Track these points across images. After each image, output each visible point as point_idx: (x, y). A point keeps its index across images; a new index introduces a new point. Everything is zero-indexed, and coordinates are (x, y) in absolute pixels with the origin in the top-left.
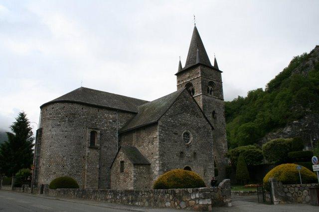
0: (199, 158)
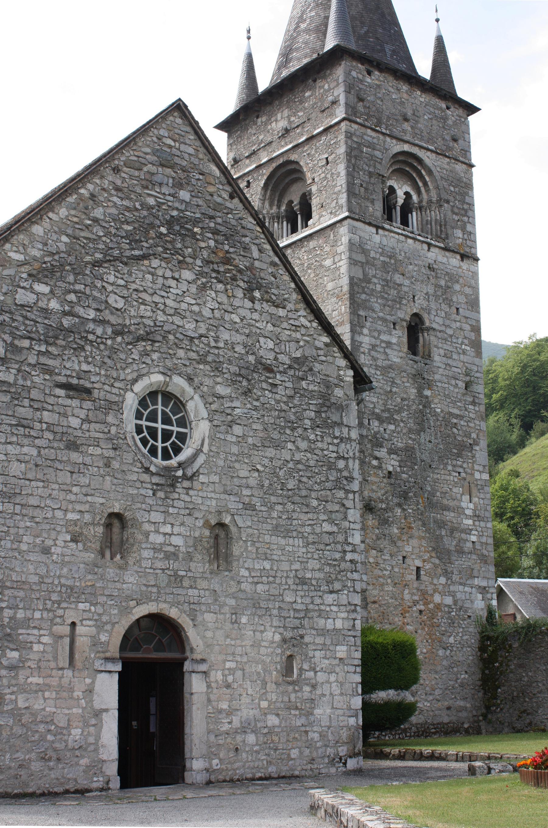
0: (247, 564)
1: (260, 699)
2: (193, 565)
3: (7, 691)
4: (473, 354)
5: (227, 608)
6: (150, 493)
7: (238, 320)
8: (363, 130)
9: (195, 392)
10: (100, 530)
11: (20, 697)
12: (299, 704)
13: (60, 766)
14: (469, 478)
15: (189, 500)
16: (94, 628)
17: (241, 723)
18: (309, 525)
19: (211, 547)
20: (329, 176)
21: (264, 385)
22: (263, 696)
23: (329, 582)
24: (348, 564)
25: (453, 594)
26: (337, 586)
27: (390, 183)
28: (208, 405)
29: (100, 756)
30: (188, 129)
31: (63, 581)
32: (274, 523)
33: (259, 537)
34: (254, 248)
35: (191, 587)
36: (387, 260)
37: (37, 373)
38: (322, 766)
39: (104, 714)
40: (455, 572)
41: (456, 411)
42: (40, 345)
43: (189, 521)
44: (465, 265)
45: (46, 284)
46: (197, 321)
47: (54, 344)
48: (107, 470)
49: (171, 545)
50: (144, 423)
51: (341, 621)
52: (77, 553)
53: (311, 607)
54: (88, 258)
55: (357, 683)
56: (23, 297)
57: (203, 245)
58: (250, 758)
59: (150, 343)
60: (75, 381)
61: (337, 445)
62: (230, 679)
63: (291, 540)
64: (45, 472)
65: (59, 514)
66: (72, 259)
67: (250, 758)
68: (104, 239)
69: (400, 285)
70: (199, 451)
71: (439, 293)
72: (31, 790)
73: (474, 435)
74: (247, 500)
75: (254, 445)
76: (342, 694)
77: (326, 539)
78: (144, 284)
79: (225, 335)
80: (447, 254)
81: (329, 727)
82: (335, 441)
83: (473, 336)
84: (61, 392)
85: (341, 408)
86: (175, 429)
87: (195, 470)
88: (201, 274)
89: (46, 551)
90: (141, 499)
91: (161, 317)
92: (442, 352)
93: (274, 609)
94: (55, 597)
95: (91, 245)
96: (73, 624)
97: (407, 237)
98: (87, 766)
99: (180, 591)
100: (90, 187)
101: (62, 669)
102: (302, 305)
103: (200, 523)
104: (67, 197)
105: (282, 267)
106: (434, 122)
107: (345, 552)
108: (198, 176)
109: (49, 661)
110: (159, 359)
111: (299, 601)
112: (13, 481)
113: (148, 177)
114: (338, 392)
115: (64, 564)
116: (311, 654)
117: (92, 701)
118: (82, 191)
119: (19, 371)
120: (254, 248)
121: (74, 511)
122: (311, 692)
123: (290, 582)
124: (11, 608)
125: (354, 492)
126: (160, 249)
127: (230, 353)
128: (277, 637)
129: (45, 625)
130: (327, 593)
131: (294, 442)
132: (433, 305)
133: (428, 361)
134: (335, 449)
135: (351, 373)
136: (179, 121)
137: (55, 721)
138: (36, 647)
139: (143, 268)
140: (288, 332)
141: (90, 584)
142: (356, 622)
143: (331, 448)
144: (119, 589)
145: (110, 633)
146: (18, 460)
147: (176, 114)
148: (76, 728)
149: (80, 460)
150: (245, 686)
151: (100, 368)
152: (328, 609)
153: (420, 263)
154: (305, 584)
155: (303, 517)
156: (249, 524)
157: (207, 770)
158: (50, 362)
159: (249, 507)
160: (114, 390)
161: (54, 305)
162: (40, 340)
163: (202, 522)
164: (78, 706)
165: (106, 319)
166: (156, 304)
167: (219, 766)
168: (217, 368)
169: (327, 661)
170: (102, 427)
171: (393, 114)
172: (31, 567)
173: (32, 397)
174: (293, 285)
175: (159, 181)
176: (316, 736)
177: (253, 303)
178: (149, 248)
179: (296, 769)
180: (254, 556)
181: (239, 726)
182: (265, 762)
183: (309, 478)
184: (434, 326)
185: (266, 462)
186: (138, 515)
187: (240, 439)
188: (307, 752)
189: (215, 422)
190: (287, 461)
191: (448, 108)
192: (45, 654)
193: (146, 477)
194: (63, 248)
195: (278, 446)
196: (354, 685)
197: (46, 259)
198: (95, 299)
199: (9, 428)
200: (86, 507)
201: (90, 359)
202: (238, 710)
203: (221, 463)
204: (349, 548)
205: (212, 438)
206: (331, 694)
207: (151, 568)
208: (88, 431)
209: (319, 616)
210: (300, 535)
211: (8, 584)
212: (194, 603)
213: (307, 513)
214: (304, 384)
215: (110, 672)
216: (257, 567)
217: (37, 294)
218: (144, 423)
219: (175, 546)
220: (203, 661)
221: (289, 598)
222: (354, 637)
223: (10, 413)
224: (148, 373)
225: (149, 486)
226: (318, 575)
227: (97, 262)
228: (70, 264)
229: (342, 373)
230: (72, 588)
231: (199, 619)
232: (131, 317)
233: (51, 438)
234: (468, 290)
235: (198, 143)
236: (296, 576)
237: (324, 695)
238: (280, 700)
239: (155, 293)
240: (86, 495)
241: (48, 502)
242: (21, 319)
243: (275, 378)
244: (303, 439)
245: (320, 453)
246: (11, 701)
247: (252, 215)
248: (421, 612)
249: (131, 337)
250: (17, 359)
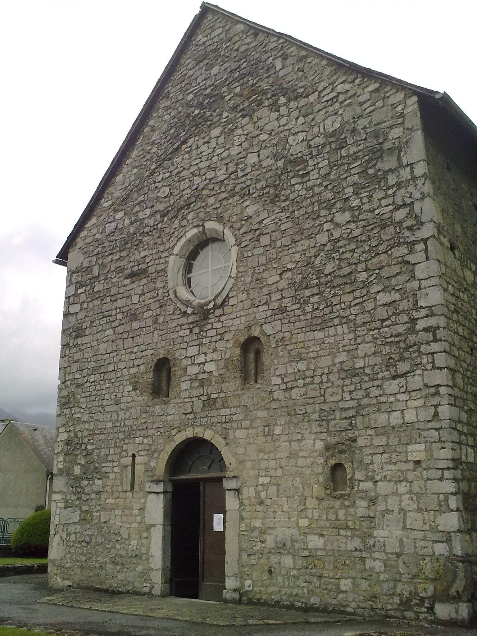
1: (299, 517)
6: (188, 332)
12: (350, 523)
13: (125, 570)
16: (146, 457)
17: (276, 542)
26: (403, 367)
31: (127, 423)
33: (290, 339)
38: (390, 607)
39: (152, 528)
43: (220, 345)
49: (205, 372)
51: (414, 412)
53: (366, 401)
58: (287, 583)
60: (135, 269)
63: (332, 331)
67: (287, 583)
72: (105, 587)
77: (382, 313)
81: (398, 555)
82: (390, 192)
84: (127, 281)
87: (224, 297)
90: (180, 340)
93: (314, 413)
99: (213, 413)
101: (125, 492)
107: (413, 321)
109: (118, 486)
116: (367, 460)
121: (134, 366)
122: (368, 507)
125: (425, 241)
128: (320, 445)
130: (388, 379)
138: (112, 476)
142: (439, 409)
148: (133, 540)
150: (280, 503)
152: (392, 399)
155: (347, 298)
156: (278, 328)
167: (251, 588)
168: (244, 194)
169: (393, 467)
176: (378, 566)
182: (306, 590)
183: (353, 251)
186: (177, 355)
188: (365, 585)
190: (325, 245)
193: (184, 320)
196: (442, 497)
200: (142, 361)
203: (249, 279)
207: (188, 398)
209: (379, 410)
210: (344, 321)
211: (96, 432)
212: (226, 422)
215: (157, 493)
216: (290, 370)
222: (436, 429)
226: (372, 361)
231: (231, 436)
238: (324, 517)
240: (142, 351)
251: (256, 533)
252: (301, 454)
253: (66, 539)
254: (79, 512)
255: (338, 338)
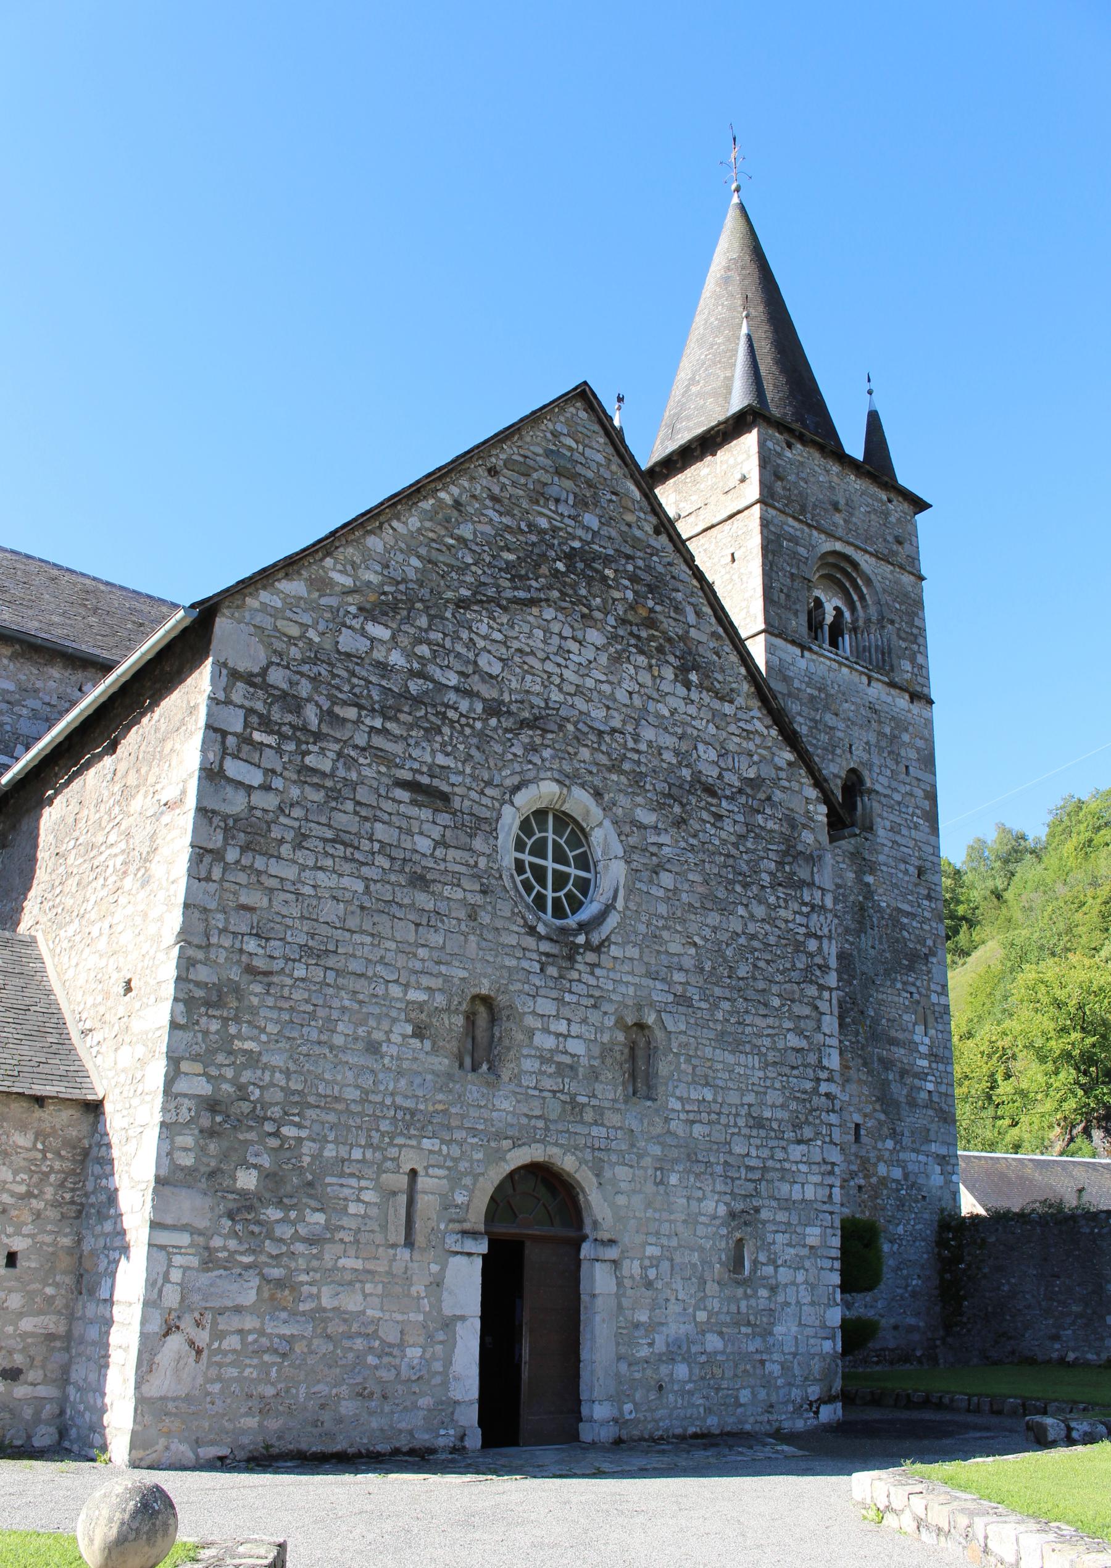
0: (678, 1092)
1: (697, 1308)
2: (599, 1088)
3: (303, 1278)
4: (927, 830)
5: (649, 1159)
7: (667, 714)
8: (782, 517)
9: (605, 816)
10: (459, 1021)
11: (324, 1289)
12: (752, 1318)
14: (923, 1001)
15: (594, 983)
16: (445, 1181)
17: (668, 1345)
18: (768, 1035)
19: (626, 1061)
20: (735, 577)
21: (705, 815)
22: (700, 1304)
23: (797, 1126)
24: (823, 1099)
25: (902, 1163)
26: (808, 1132)
27: (817, 593)
28: (623, 838)
29: (451, 1394)
30: (597, 427)
31: (399, 1100)
32: (719, 1028)
33: (696, 1049)
34: (689, 610)
35: (596, 1123)
36: (816, 693)
37: (368, 761)
40: (907, 1134)
41: (906, 907)
42: (373, 718)
43: (594, 1017)
44: (916, 708)
45: (387, 626)
46: (608, 708)
47: (397, 720)
48: (472, 924)
49: (566, 1053)
50: (527, 858)
51: (812, 1187)
52: (422, 1056)
53: (770, 1163)
54: (449, 595)
55: (835, 1287)
56: (348, 641)
57: (617, 595)
58: (680, 1401)
59: (539, 732)
60: (425, 780)
61: (807, 916)
62: (652, 1273)
63: (743, 1057)
64: (376, 919)
65: (395, 991)
66: (424, 592)
67: (680, 1401)
68: (474, 568)
69: (832, 728)
70: (608, 908)
71: (883, 744)
72: (338, 1448)
73: (929, 942)
74: (679, 990)
75: (690, 905)
76: (812, 1304)
77: (792, 1058)
78: (532, 643)
79: (648, 733)
80: (893, 691)
81: (795, 1355)
82: (805, 909)
83: (926, 805)
84: (404, 795)
85: (812, 859)
86: (573, 871)
88: (614, 638)
89: (373, 1048)
91: (556, 696)
92: (888, 824)
94: (385, 1126)
95: (453, 574)
96: (413, 1173)
97: (840, 664)
98: (429, 1410)
99: (579, 1129)
100: (455, 491)
101: (394, 1246)
102: (755, 703)
103: (610, 1022)
104: (420, 501)
105: (728, 642)
106: (873, 517)
107: (818, 1080)
108: (608, 497)
109: (372, 1231)
110: (553, 757)
111: (754, 1153)
112: (324, 930)
113: (538, 487)
114: (808, 837)
115: (400, 1073)
116: (770, 1238)
117: (440, 1301)
118: (442, 495)
119: (340, 754)
120: (689, 610)
122: (769, 1298)
123: (741, 1122)
124: (314, 1141)
125: (831, 989)
126: (555, 594)
127: (655, 762)
128: (722, 1210)
129: (369, 1172)
130: (793, 1142)
131: (746, 906)
132: (876, 761)
133: (869, 836)
134: (804, 921)
135: (823, 809)
136: (583, 415)
137: (381, 1333)
138: (353, 1208)
139: (531, 619)
140: (736, 740)
141: (440, 1107)
143: (799, 919)
144: (486, 1120)
145: (472, 1192)
146: (334, 898)
147: (578, 404)
148: (413, 1346)
149: (430, 906)
150: (674, 1286)
151: (464, 763)
153: (858, 700)
154: (763, 1127)
155: (759, 1021)
156: (683, 1027)
157: (615, 1421)
158: (389, 746)
159: (682, 1000)
160: (485, 801)
161: (396, 658)
162: (373, 710)
163: (613, 1018)
164: (419, 1310)
165: (475, 689)
166: (550, 675)
169: (792, 1251)
170: (466, 855)
171: (820, 501)
172: (350, 1074)
173: (358, 798)
174: (743, 671)
175: (554, 495)
176: (776, 1369)
177: (689, 690)
178: (539, 590)
179: (746, 1422)
180: (690, 1079)
181: (664, 1349)
182: (702, 1410)
183: (768, 962)
184: (878, 787)
185: (707, 932)
186: (518, 1004)
187: (670, 894)
188: (762, 1394)
189: (634, 865)
191: (890, 501)
192: (367, 1220)
193: (530, 942)
194: (411, 575)
195: (725, 910)
197: (386, 589)
198: (458, 655)
199: (321, 845)
201: (449, 749)
202: (662, 1324)
204: (824, 1075)
205: (630, 891)
206: (798, 1302)
207: (535, 1088)
208: (444, 860)
209: (782, 1179)
211: (311, 1099)
212: (599, 1149)
213: (765, 1016)
214: (760, 819)
215: (469, 1254)
216: (694, 1095)
217: (372, 640)
218: (527, 858)
219: (573, 1056)
220: (612, 1242)
221: (739, 1149)
222: (831, 1213)
223: (323, 820)
224: (536, 780)
225: (535, 956)
226: (780, 1114)
227: (463, 601)
228: (421, 600)
229: (811, 807)
230: (413, 1114)
231: (608, 1174)
232: (511, 691)
233: (387, 866)
234: (920, 743)
235: (610, 450)
236: (749, 1114)
237: (787, 1304)
238: (725, 1310)
239: (548, 658)
240: (439, 963)
241: (379, 968)
242: (345, 674)
243: (719, 806)
244: (760, 902)
245: (783, 926)
246: (311, 1296)
247: (686, 561)
248: (860, 1187)
249: (511, 720)
250: (338, 735)
251: (642, 1332)
252: (702, 1219)
253: (209, 1345)
254: (255, 1282)
255: (749, 1072)
